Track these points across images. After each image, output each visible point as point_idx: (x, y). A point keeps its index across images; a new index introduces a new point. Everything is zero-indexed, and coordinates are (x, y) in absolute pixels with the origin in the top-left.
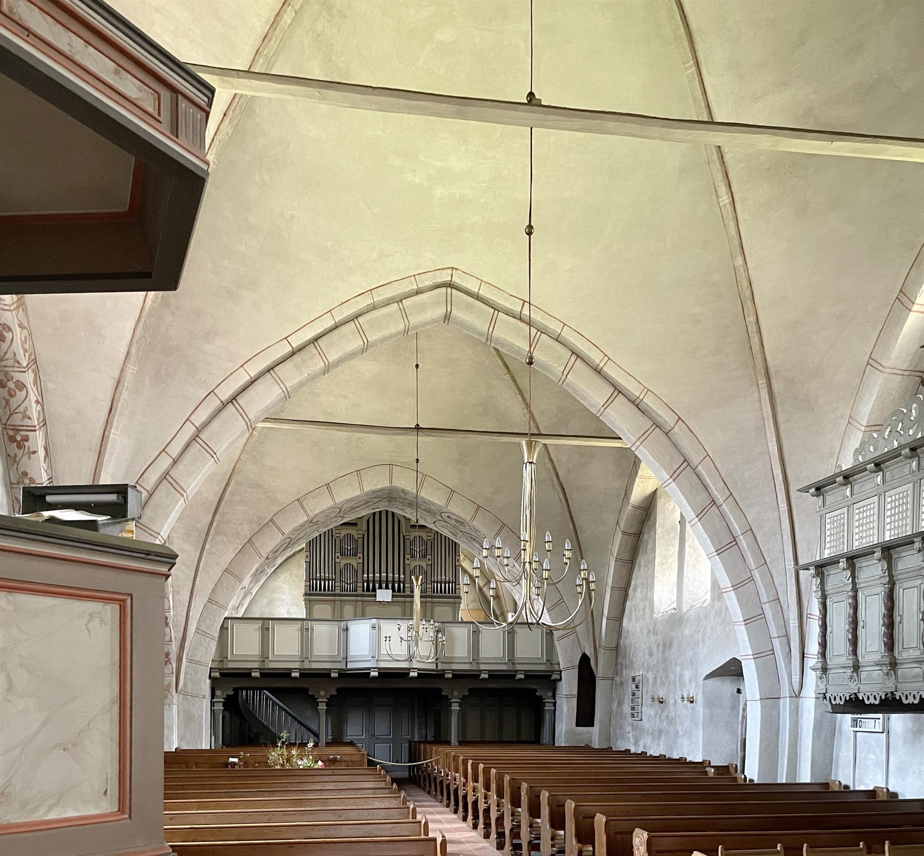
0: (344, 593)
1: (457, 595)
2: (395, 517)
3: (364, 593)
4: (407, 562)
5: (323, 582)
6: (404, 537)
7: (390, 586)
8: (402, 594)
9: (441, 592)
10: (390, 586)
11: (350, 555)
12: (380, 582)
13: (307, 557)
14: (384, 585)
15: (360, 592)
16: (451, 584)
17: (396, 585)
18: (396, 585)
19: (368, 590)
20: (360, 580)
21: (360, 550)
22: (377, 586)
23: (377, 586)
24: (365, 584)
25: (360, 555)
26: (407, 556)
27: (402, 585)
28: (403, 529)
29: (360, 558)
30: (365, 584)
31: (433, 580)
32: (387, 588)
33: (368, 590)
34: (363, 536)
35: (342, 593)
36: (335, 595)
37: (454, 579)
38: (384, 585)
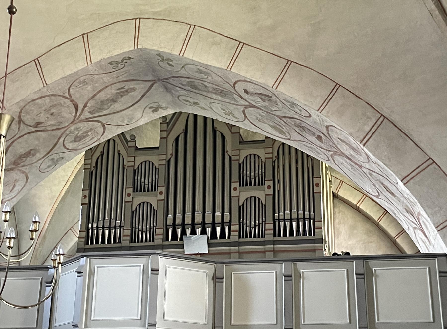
0: (136, 244)
1: (317, 237)
2: (218, 133)
3: (166, 243)
4: (234, 193)
5: (107, 232)
6: (230, 157)
7: (209, 230)
8: (227, 240)
9: (291, 234)
10: (209, 230)
11: (148, 190)
12: (193, 226)
13: (85, 197)
14: (198, 231)
15: (158, 240)
16: (307, 222)
17: (218, 230)
18: (218, 230)
19: (174, 237)
20: (160, 223)
21: (162, 181)
22: (188, 231)
23: (188, 231)
24: (170, 230)
25: (163, 189)
26: (233, 185)
27: (227, 228)
28: (228, 147)
29: (161, 193)
30: (170, 230)
31: (276, 218)
32: (204, 232)
33: (174, 237)
34: (169, 161)
35: (133, 244)
36: (120, 249)
37: (312, 213)
38: (198, 231)
